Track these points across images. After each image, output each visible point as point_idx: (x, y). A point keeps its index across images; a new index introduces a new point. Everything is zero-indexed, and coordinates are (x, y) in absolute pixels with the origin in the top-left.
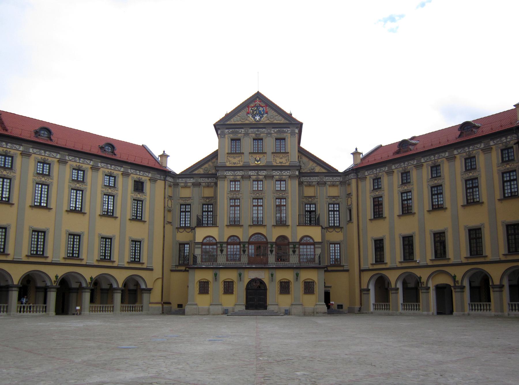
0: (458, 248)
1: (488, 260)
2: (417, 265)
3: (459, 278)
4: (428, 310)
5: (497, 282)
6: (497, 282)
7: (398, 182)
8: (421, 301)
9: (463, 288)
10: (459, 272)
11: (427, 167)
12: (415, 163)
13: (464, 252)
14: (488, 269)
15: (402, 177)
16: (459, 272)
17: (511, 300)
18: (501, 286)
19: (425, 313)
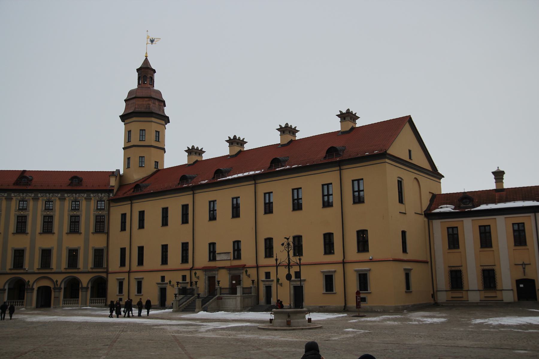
0: (59, 262)
1: (80, 271)
2: (25, 272)
3: (59, 283)
4: (31, 305)
5: (85, 285)
6: (85, 285)
7: (16, 208)
8: (25, 298)
9: (60, 288)
10: (59, 278)
11: (42, 201)
12: (33, 195)
13: (64, 264)
14: (80, 277)
15: (19, 204)
16: (59, 278)
17: (91, 297)
18: (87, 288)
19: (29, 307)
